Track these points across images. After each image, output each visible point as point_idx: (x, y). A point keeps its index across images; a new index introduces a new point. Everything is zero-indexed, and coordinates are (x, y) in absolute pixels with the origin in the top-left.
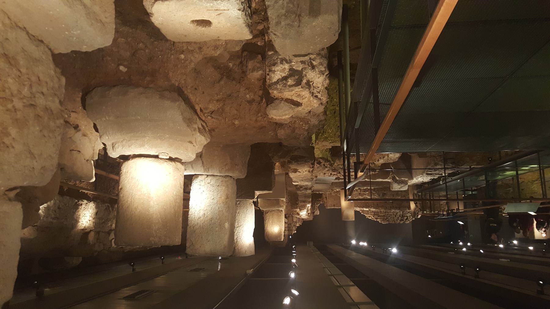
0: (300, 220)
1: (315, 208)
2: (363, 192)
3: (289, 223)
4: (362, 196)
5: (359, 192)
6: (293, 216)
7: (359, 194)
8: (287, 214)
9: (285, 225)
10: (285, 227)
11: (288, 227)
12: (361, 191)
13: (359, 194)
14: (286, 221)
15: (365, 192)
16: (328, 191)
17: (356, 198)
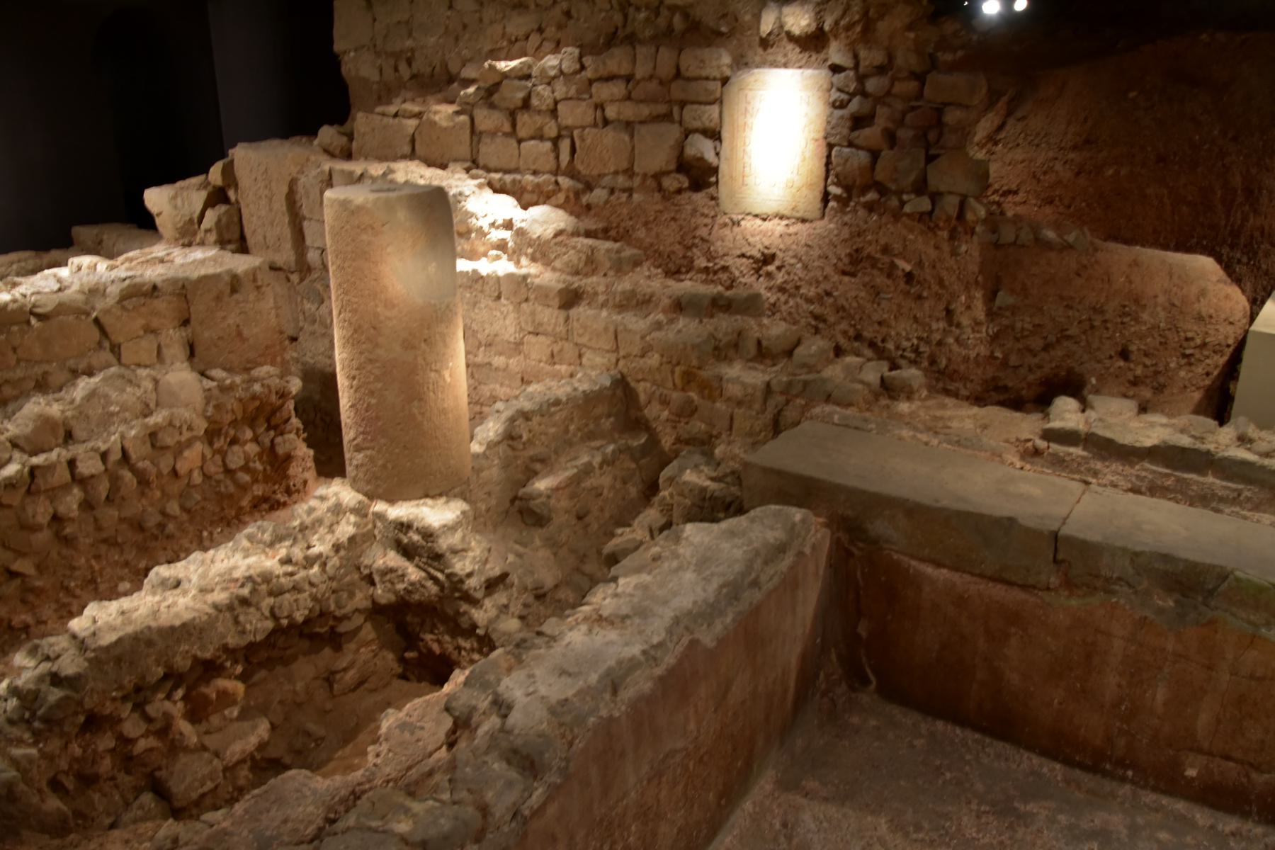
0: (407, 149)
1: (220, 234)
2: (50, 468)
3: (674, 132)
4: (46, 423)
5: (78, 450)
6: (565, 182)
7: (69, 437)
8: (679, 191)
9: (721, 113)
10: (720, 101)
11: (683, 104)
12: (72, 463)
13: (69, 437)
14: (705, 148)
15: (33, 471)
16: (536, 419)
17: (92, 395)
